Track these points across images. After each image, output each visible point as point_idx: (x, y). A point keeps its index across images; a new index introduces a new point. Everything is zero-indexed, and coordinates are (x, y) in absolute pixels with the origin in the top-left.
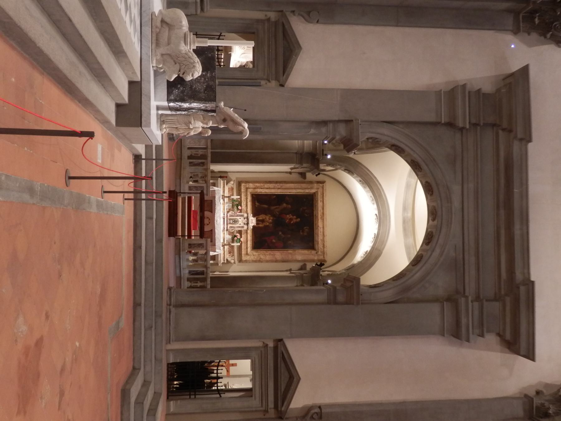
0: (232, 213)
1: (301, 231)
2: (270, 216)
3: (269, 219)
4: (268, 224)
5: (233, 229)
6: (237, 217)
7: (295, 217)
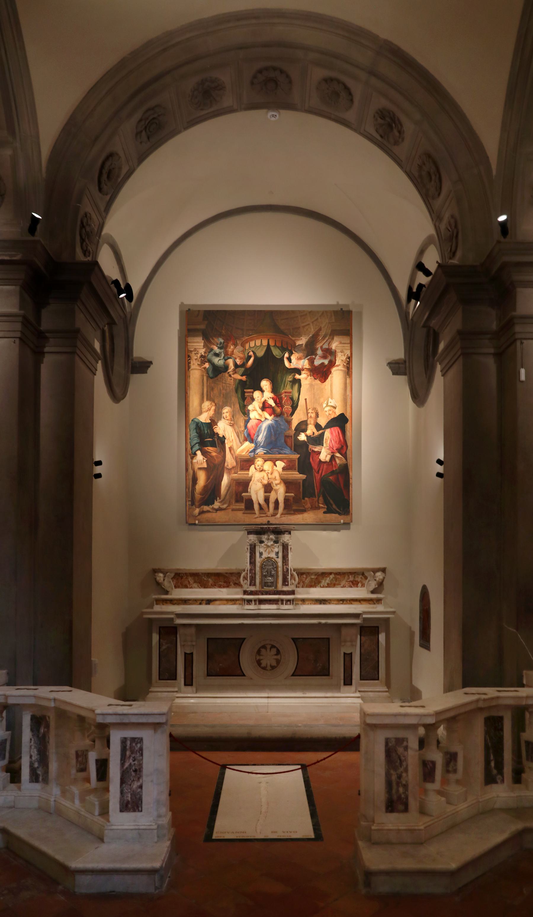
0: (245, 578)
2: (253, 467)
5: (292, 575)
6: (258, 564)
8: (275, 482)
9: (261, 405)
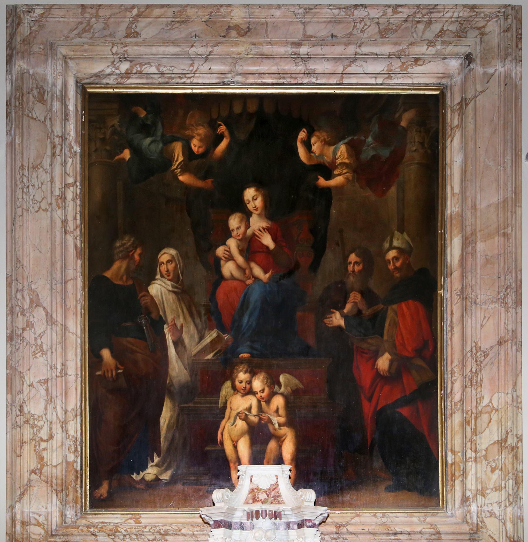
1: (322, 182)
3: (250, 392)
4: (278, 401)
7: (234, 222)
8: (276, 420)
9: (245, 245)
